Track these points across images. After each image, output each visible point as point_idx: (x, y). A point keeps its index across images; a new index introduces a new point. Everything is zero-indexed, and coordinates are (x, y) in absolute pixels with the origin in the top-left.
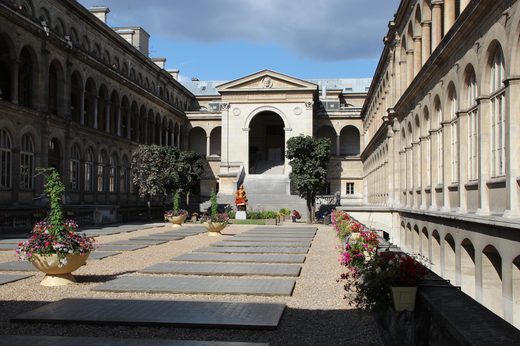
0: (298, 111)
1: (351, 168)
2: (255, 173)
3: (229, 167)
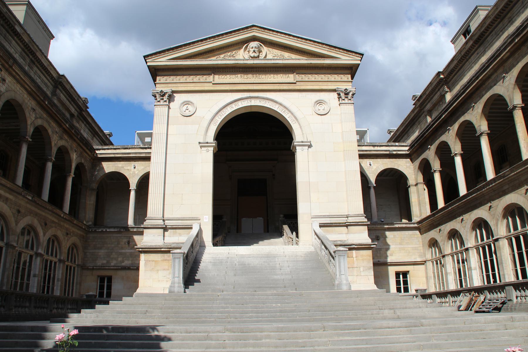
0: (322, 109)
1: (400, 244)
2: (224, 244)
3: (165, 229)
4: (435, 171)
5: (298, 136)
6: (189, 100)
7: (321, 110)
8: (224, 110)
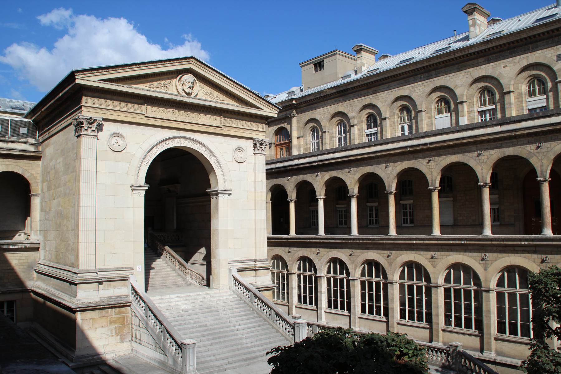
0: (240, 155)
4: (291, 201)
6: (118, 131)
7: (239, 158)
8: (155, 148)
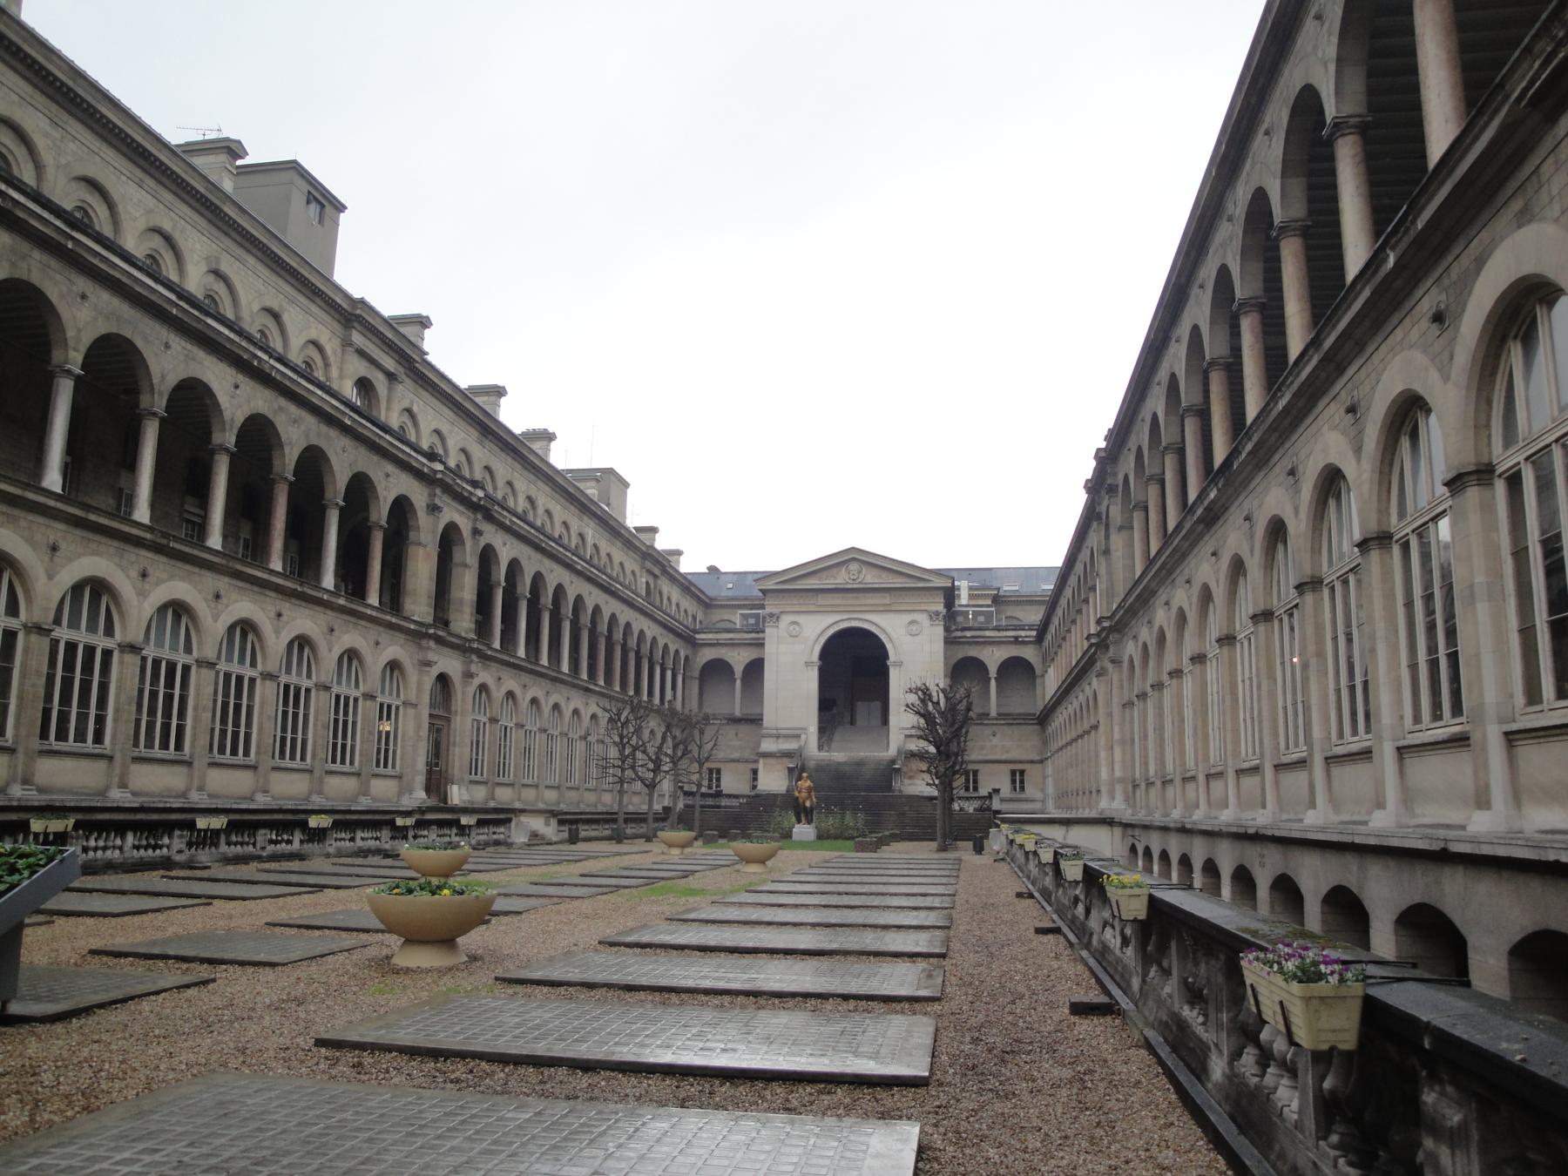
0: (914, 628)
5: (892, 657)
